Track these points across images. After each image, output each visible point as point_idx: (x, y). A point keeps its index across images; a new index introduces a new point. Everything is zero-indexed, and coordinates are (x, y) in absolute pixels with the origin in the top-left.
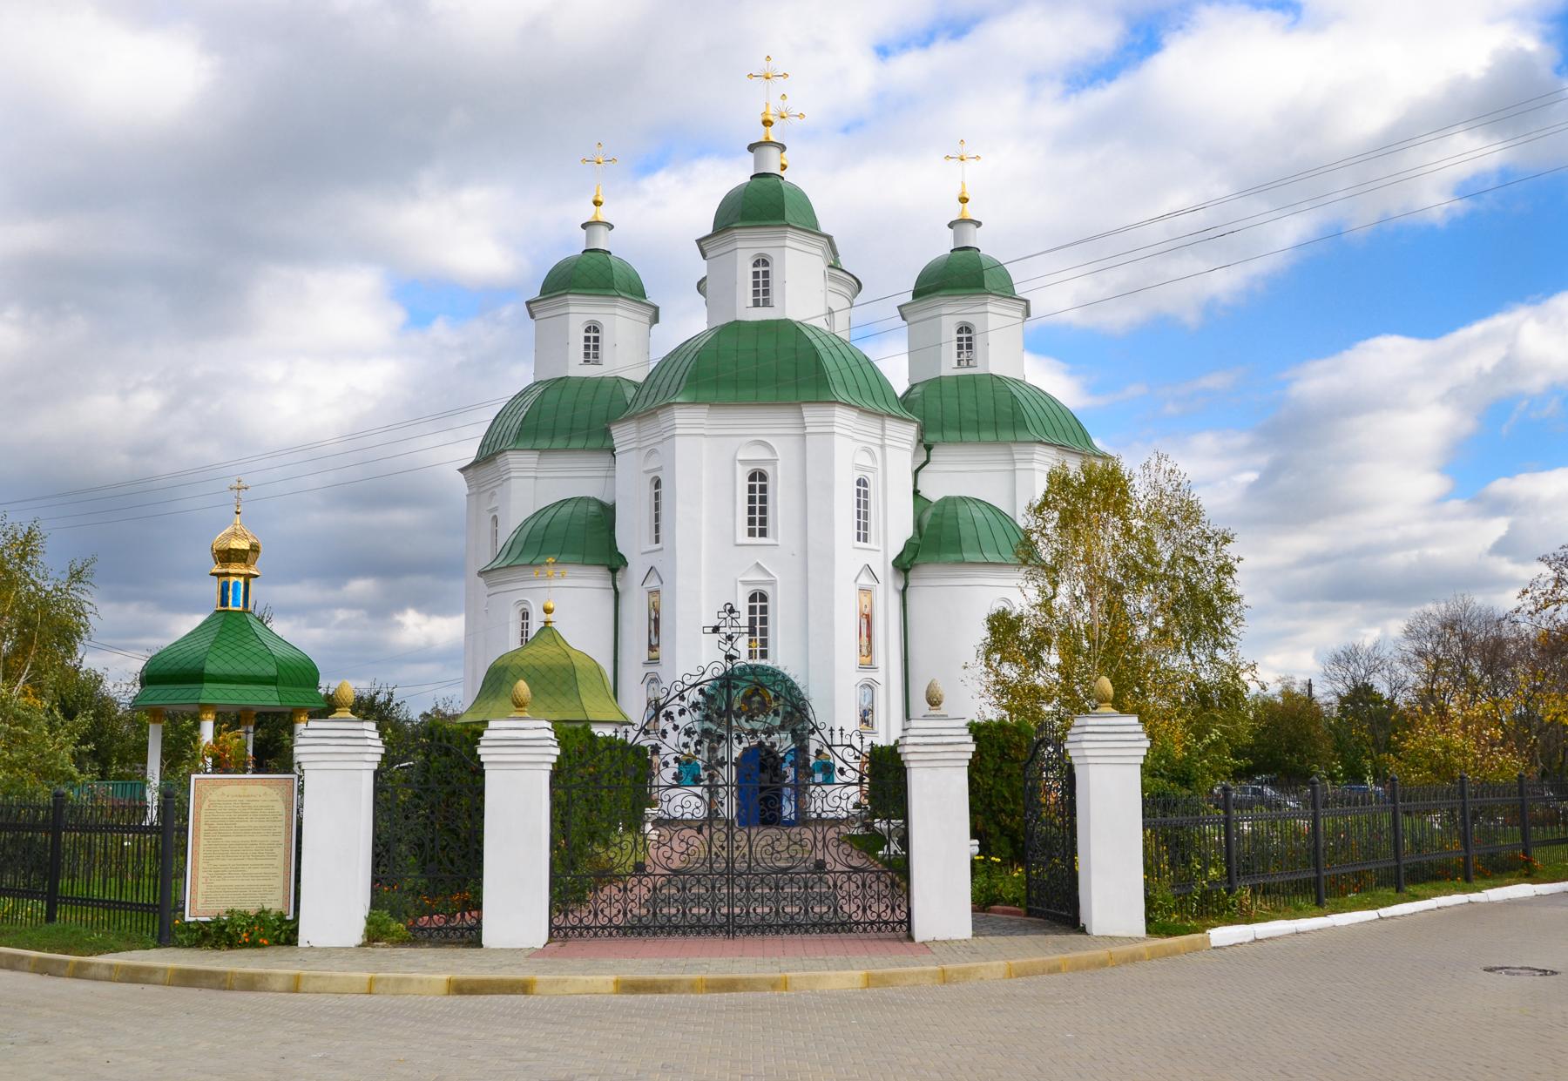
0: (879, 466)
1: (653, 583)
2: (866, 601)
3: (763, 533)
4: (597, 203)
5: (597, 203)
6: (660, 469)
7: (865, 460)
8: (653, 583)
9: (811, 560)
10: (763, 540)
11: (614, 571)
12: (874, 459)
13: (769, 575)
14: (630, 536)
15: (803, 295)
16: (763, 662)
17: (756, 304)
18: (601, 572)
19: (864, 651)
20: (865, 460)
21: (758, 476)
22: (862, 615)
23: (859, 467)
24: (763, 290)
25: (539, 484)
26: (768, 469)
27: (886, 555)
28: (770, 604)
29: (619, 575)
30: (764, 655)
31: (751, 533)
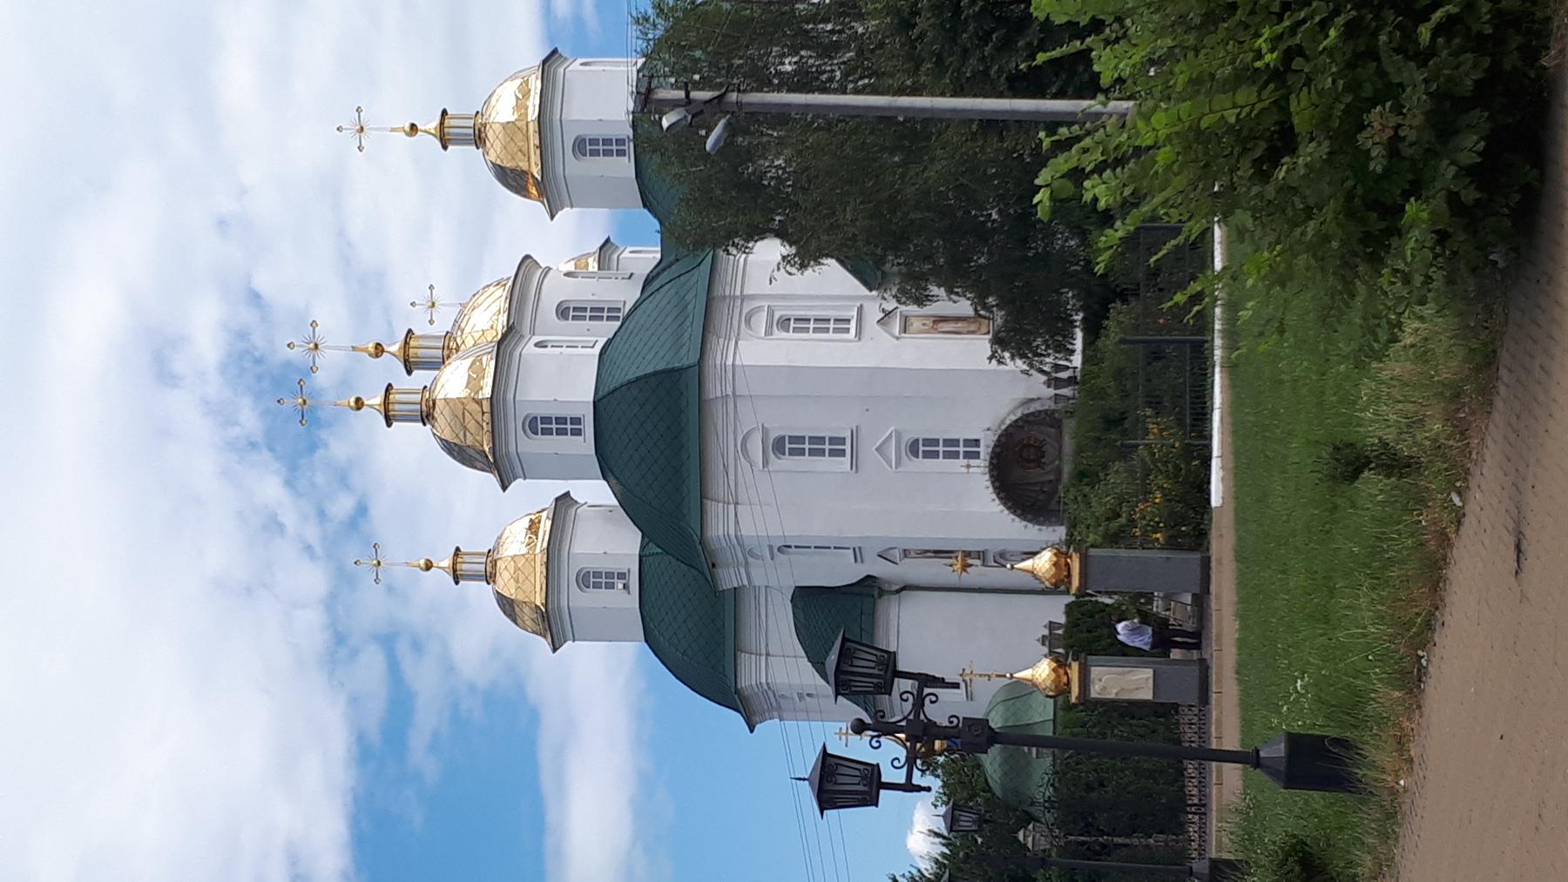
0: (766, 304)
1: (897, 554)
2: (916, 324)
3: (842, 441)
4: (428, 566)
5: (428, 566)
6: (771, 547)
7: (761, 320)
8: (897, 554)
9: (874, 385)
10: (848, 442)
11: (882, 592)
12: (760, 308)
13: (890, 436)
14: (840, 572)
15: (565, 374)
16: (982, 443)
17: (577, 432)
18: (882, 605)
19: (973, 328)
20: (761, 320)
21: (779, 446)
22: (934, 330)
23: (769, 332)
24: (564, 425)
25: (778, 656)
26: (773, 435)
27: (865, 297)
28: (922, 436)
29: (886, 587)
30: (977, 442)
31: (842, 453)
